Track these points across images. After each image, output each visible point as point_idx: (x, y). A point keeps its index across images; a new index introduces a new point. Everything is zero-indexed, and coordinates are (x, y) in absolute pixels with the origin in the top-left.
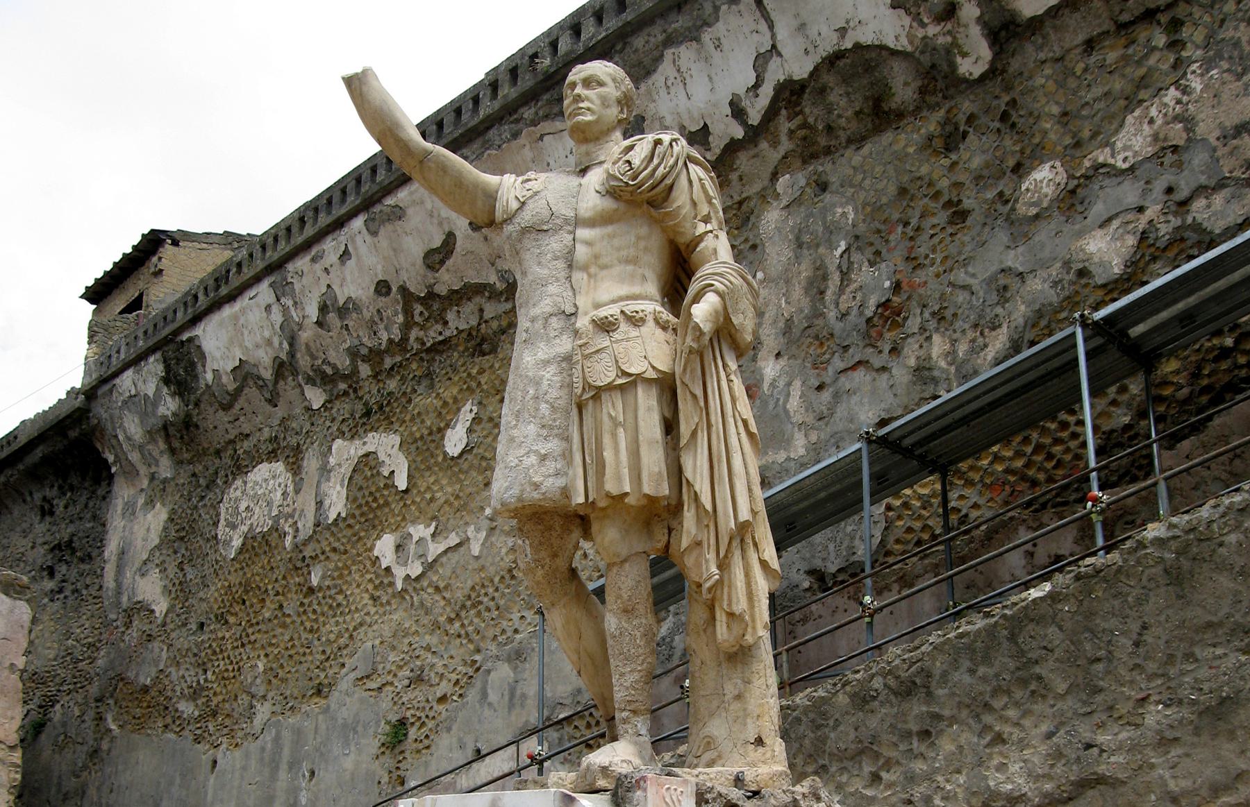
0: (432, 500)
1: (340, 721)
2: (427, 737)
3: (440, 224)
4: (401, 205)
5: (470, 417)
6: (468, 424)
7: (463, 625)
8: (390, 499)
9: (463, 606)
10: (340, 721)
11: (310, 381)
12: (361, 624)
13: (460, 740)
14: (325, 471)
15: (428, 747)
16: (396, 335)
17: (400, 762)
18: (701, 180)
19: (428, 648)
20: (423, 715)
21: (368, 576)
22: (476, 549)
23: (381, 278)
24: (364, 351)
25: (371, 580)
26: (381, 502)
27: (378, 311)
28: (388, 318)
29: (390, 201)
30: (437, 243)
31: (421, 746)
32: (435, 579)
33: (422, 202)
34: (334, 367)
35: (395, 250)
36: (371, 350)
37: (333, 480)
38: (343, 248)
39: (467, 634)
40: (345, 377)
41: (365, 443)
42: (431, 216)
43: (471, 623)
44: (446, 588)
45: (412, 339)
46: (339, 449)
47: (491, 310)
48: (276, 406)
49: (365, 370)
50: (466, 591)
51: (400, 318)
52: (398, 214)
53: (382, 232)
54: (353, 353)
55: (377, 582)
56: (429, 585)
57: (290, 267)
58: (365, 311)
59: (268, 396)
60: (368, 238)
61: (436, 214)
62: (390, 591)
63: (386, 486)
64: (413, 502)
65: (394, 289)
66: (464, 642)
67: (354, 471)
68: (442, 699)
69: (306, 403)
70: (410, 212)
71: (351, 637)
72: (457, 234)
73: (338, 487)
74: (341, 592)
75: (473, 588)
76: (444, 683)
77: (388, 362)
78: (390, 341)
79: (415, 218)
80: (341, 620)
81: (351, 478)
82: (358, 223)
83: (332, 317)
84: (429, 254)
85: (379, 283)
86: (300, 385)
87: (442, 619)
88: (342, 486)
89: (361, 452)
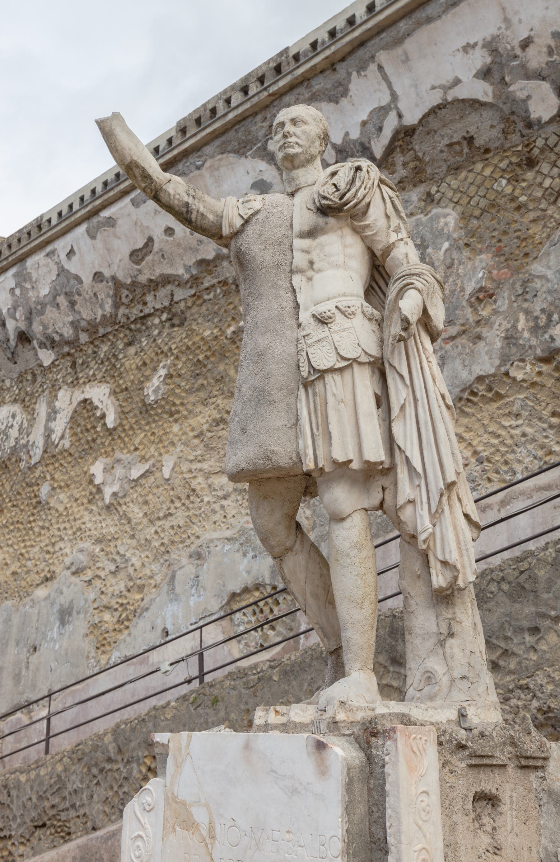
3: (142, 232)
4: (114, 217)
11: (42, 345)
14: (53, 414)
18: (390, 198)
23: (97, 270)
24: (83, 324)
28: (102, 299)
29: (105, 214)
30: (140, 245)
33: (129, 215)
34: (61, 335)
35: (108, 250)
36: (89, 323)
38: (69, 248)
40: (68, 343)
41: (83, 392)
42: (136, 224)
45: (120, 315)
47: (180, 294)
48: (16, 363)
49: (84, 338)
52: (111, 222)
53: (99, 236)
54: (75, 325)
57: (30, 262)
59: (10, 356)
60: (89, 241)
61: (139, 223)
64: (120, 437)
69: (39, 362)
70: (119, 222)
72: (155, 238)
77: (101, 331)
78: (104, 316)
79: (123, 226)
82: (82, 229)
84: (133, 253)
85: (95, 274)
86: (34, 348)
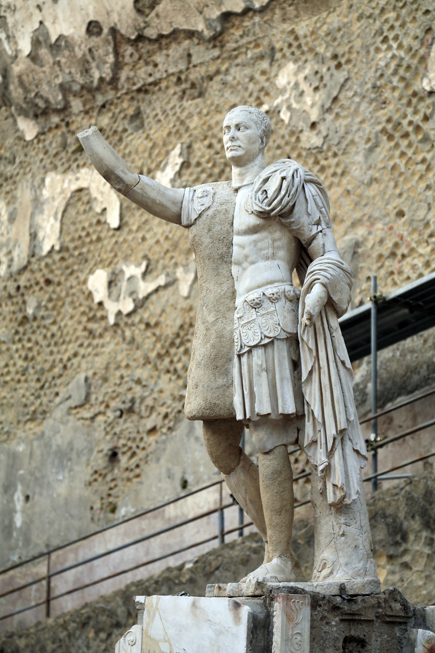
0: (144, 239)
1: (54, 448)
2: (138, 466)
5: (180, 161)
6: (177, 168)
7: (172, 362)
8: (103, 235)
9: (172, 344)
10: (54, 448)
12: (75, 355)
13: (169, 470)
15: (138, 476)
16: (107, 73)
17: (111, 489)
19: (138, 382)
20: (134, 446)
21: (82, 309)
22: (184, 290)
23: (92, 18)
25: (83, 313)
26: (94, 237)
27: (90, 50)
31: (131, 475)
32: (146, 315)
34: (47, 101)
37: (46, 212)
39: (175, 371)
41: (77, 179)
43: (179, 360)
44: (157, 324)
46: (52, 181)
50: (175, 329)
51: (111, 59)
55: (91, 315)
56: (141, 321)
58: (77, 49)
62: (103, 324)
63: (99, 222)
65: (106, 31)
66: (174, 378)
67: (68, 205)
68: (153, 430)
71: (65, 367)
73: (52, 220)
74: (54, 323)
75: (181, 327)
76: (154, 415)
80: (55, 350)
81: (64, 211)
83: (43, 52)
85: (90, 23)
87: (153, 355)
88: (56, 219)
89: (74, 187)
